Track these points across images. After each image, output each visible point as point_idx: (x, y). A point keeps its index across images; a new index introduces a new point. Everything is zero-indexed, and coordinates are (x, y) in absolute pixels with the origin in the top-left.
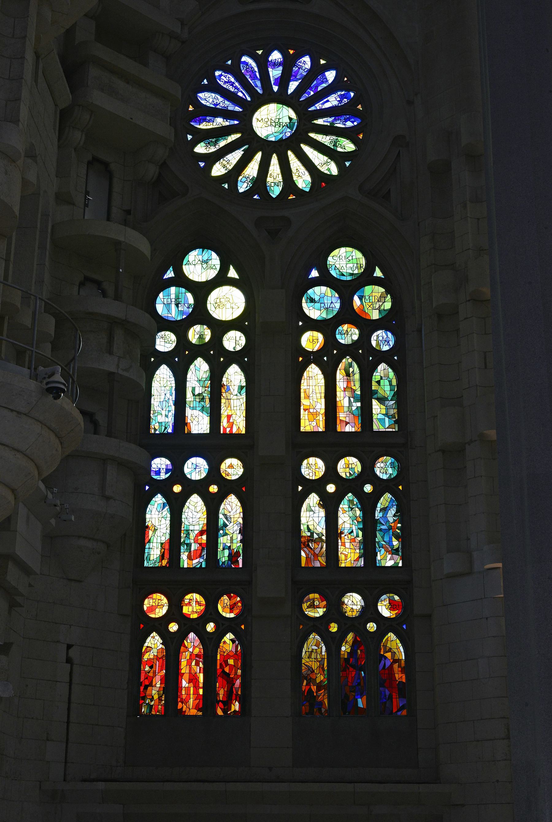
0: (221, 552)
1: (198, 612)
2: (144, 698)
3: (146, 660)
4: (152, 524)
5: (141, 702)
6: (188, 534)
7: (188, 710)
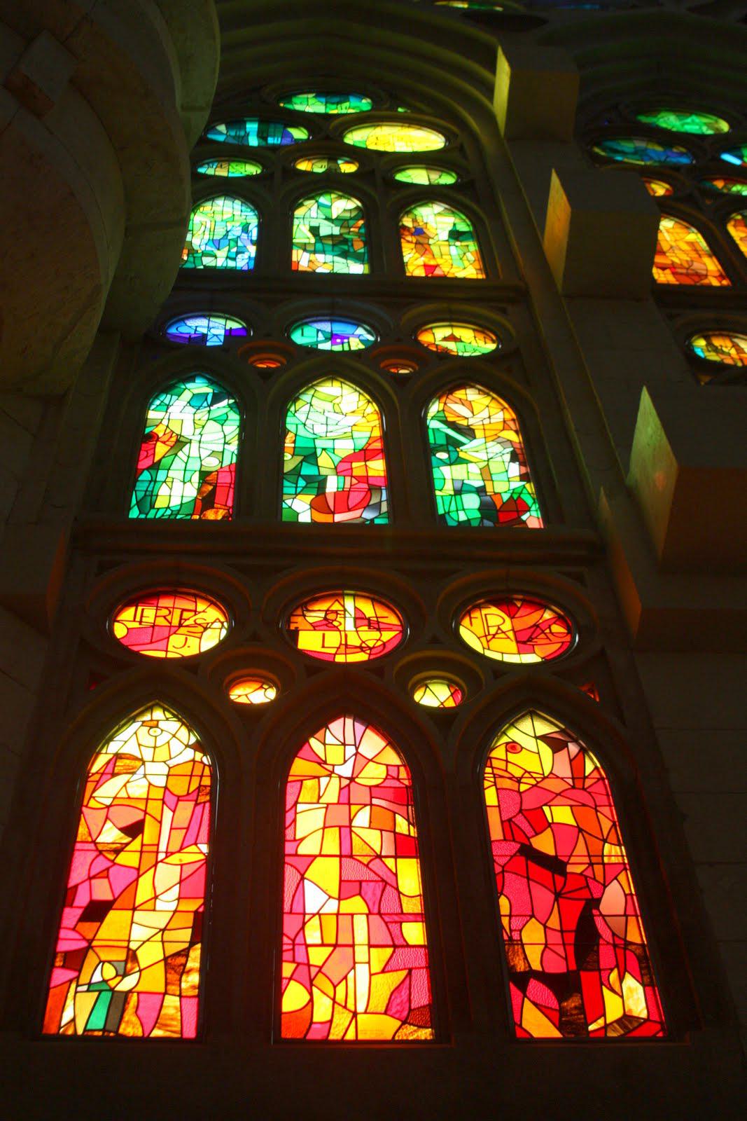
0: (447, 500)
1: (370, 649)
2: (76, 960)
3: (108, 802)
4: (168, 431)
5: (60, 976)
6: (311, 457)
7: (342, 1019)
